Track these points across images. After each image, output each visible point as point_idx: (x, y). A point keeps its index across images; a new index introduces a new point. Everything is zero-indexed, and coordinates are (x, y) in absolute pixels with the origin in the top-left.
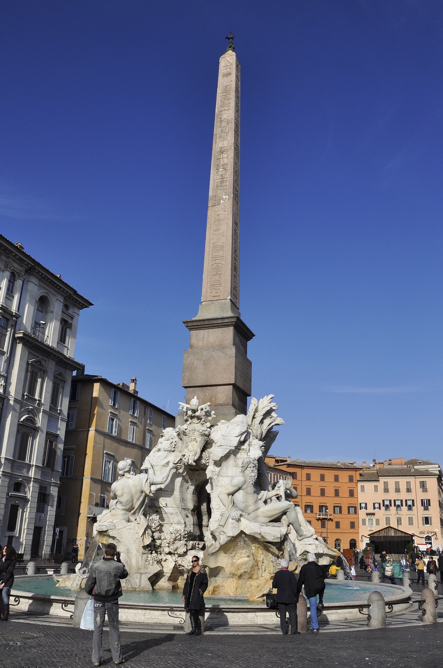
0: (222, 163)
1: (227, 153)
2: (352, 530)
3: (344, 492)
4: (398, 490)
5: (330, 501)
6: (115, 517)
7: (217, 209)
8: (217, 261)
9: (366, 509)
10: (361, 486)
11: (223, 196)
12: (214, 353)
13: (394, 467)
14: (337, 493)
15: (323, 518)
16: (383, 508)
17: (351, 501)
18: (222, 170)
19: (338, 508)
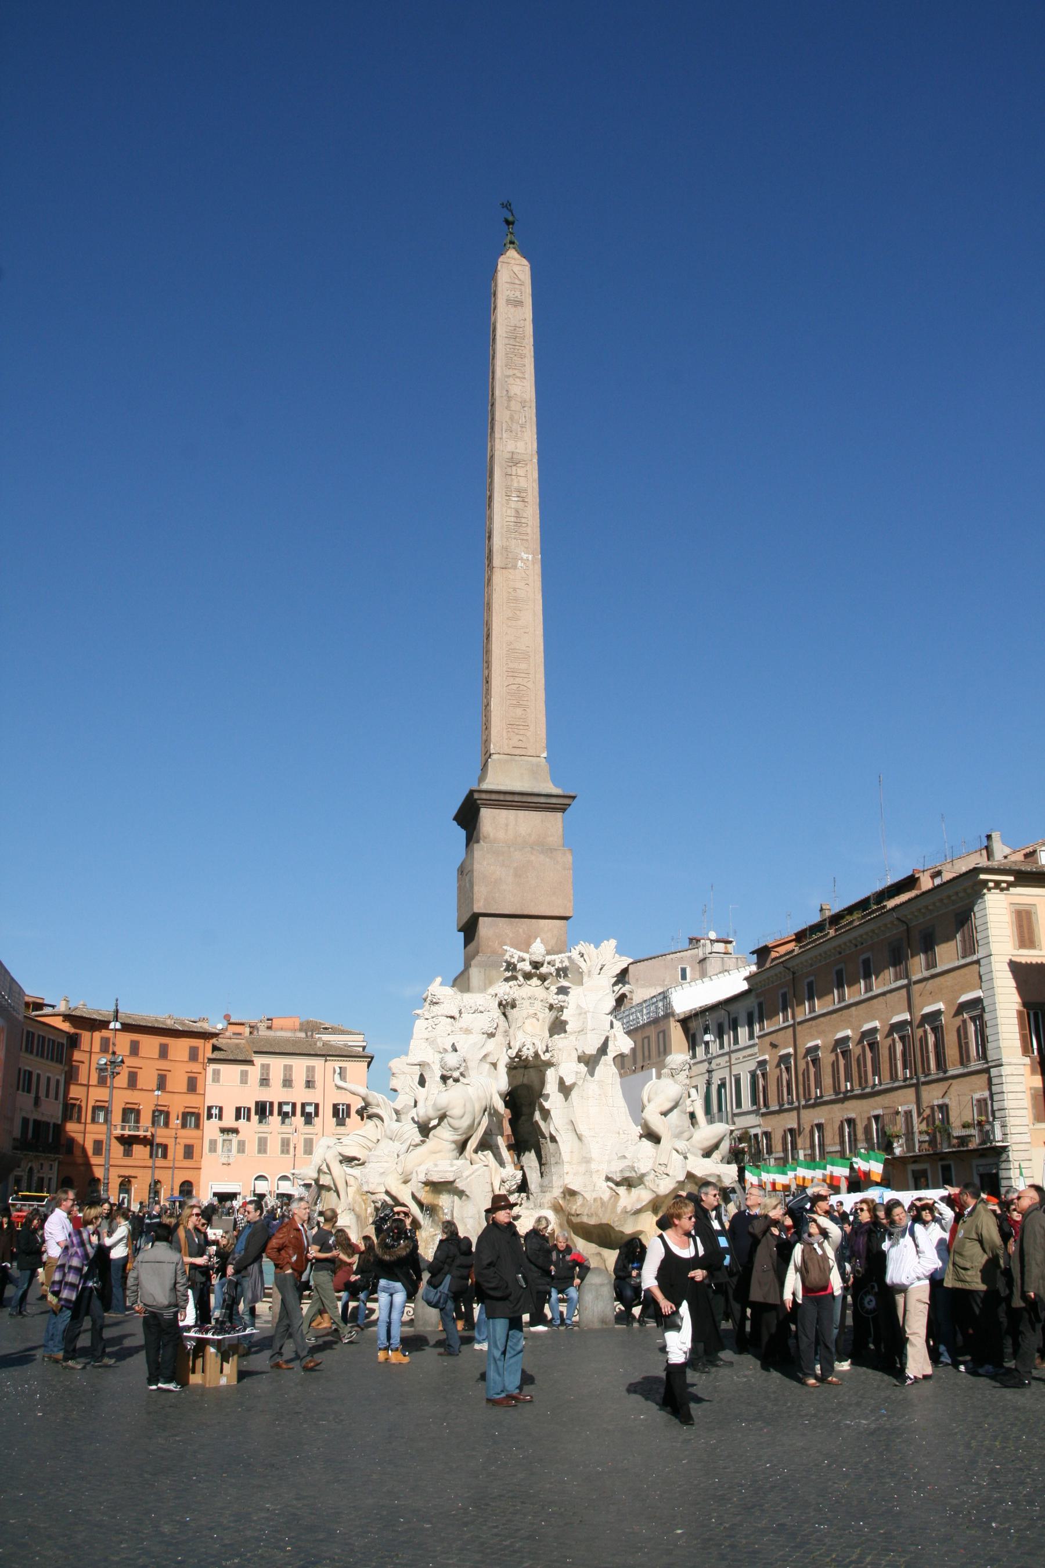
0: (515, 485)
1: (525, 469)
2: (187, 1163)
3: (177, 1081)
4: (287, 1083)
5: (146, 1102)
6: (438, 1155)
7: (511, 577)
8: (518, 680)
9: (220, 1118)
10: (214, 1070)
11: (523, 554)
12: (533, 858)
13: (279, 1034)
14: (162, 1085)
15: (130, 1136)
16: (255, 1118)
17: (191, 1101)
18: (516, 499)
19: (161, 1115)
